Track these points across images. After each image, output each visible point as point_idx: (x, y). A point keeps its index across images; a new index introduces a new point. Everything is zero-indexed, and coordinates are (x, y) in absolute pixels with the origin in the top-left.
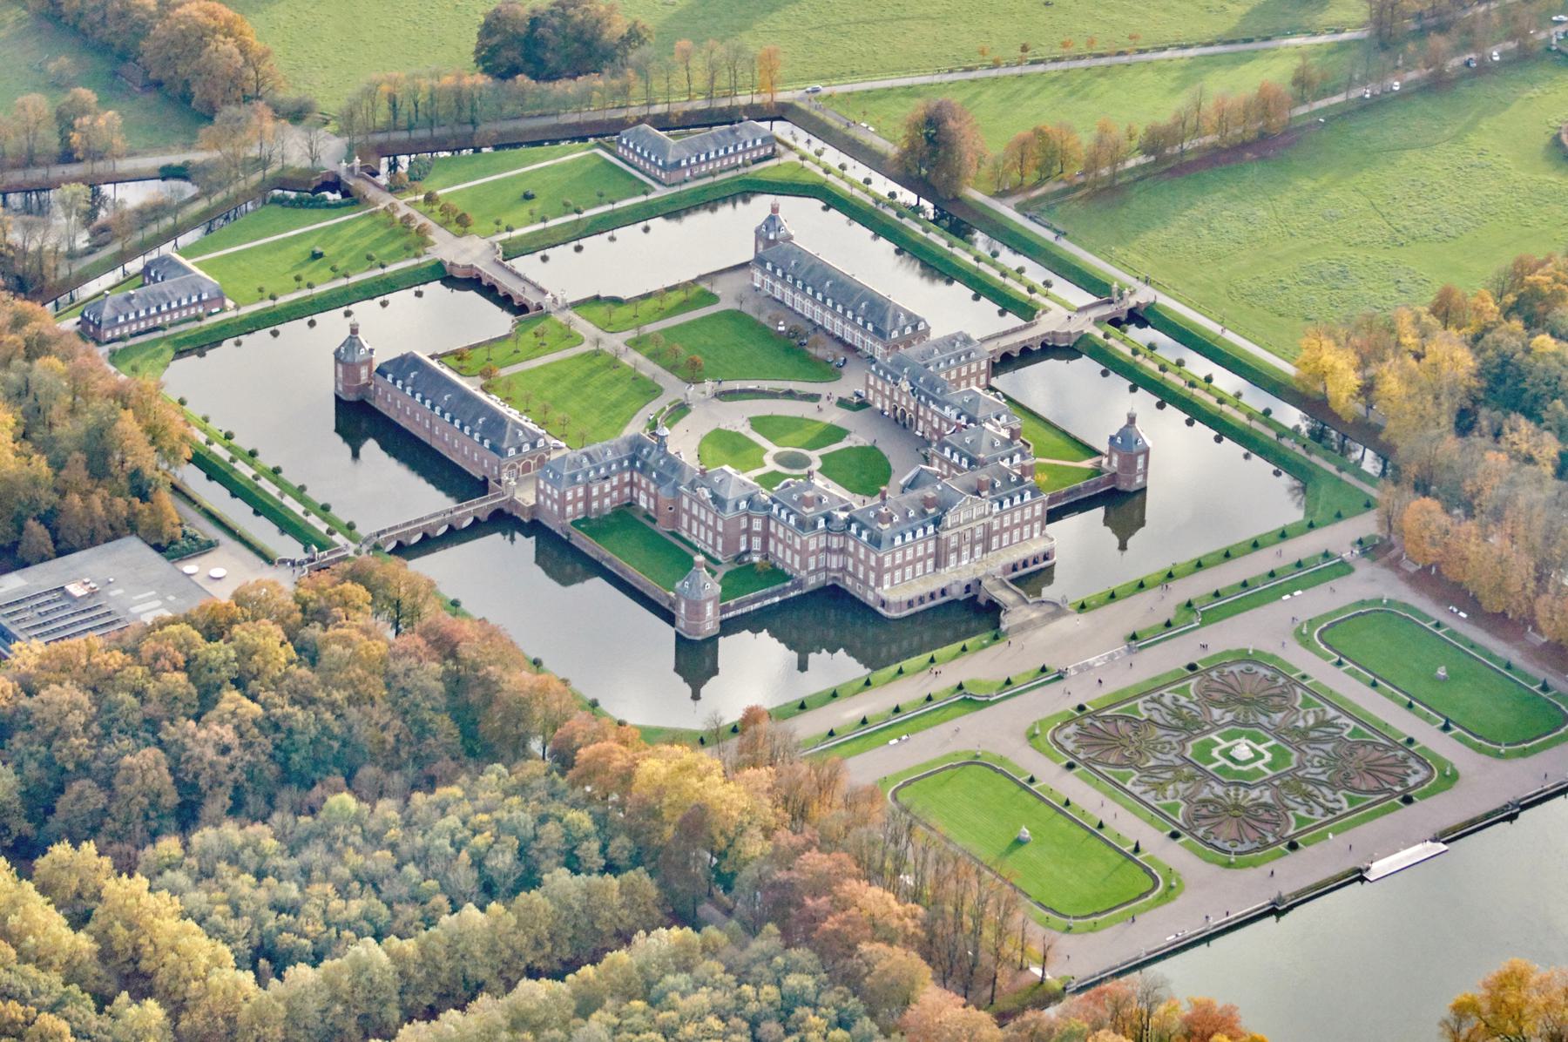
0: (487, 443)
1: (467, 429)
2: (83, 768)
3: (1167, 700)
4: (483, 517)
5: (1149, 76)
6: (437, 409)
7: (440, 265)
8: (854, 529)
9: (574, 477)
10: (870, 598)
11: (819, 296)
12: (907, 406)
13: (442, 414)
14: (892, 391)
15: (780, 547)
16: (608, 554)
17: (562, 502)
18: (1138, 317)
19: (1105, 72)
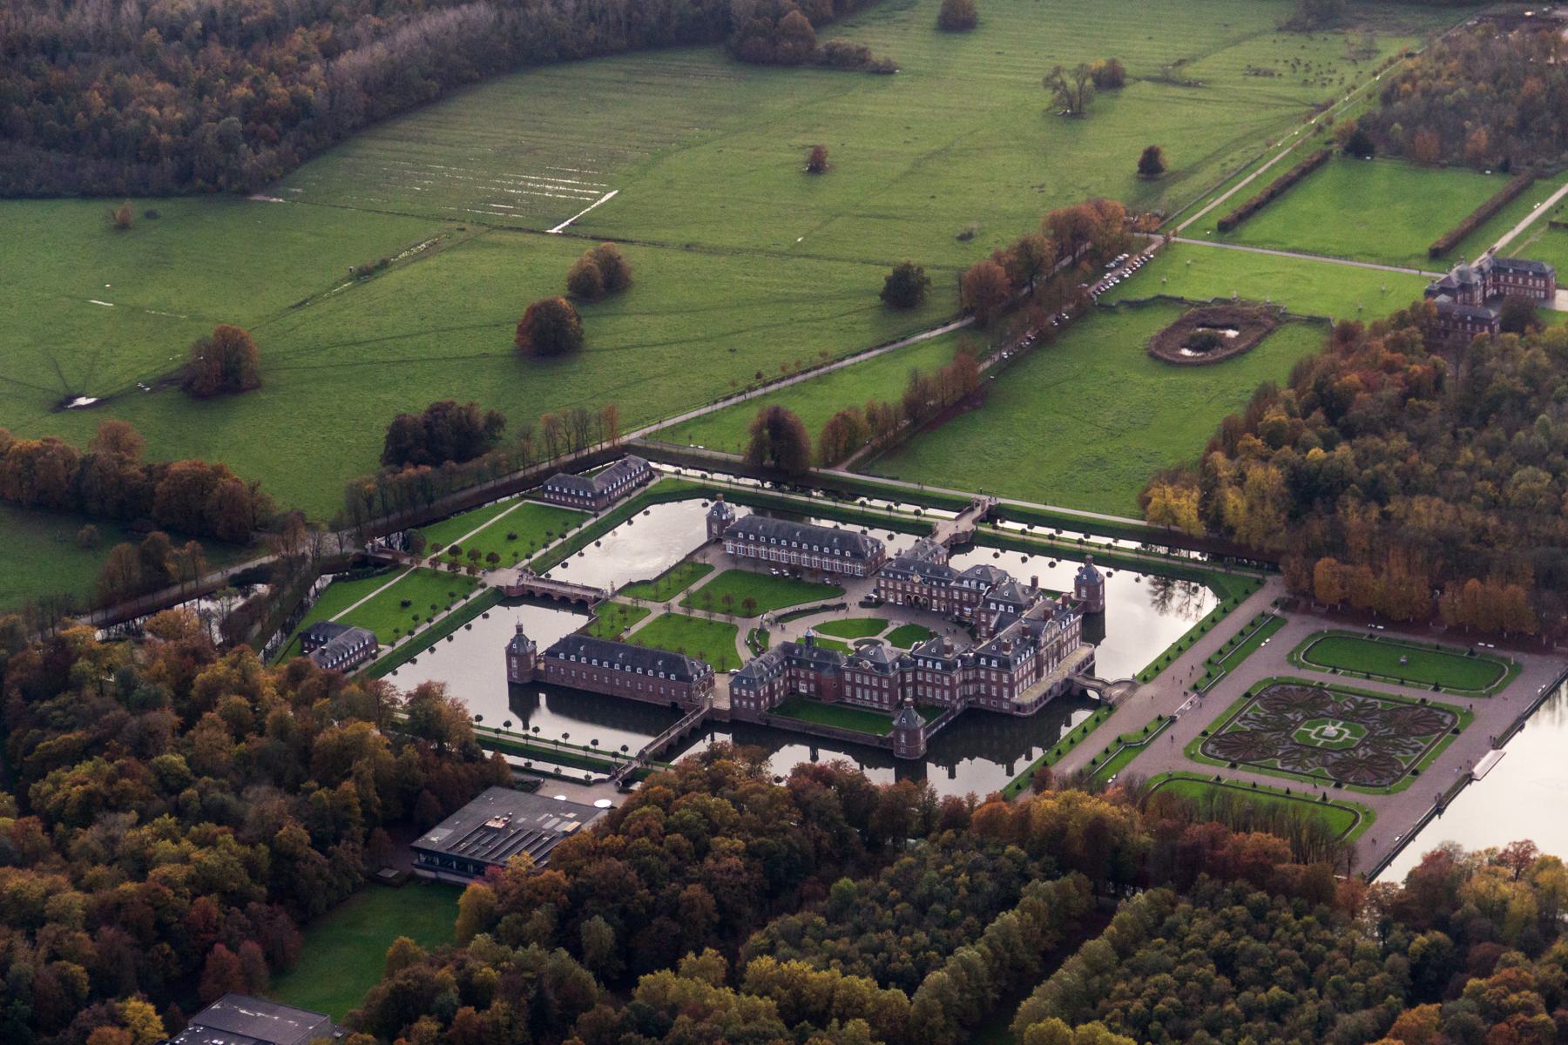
0: (673, 677)
1: (650, 673)
2: (653, 911)
3: (1250, 715)
4: (698, 725)
5: (848, 378)
6: (617, 666)
7: (498, 590)
8: (983, 661)
9: (761, 679)
10: (1006, 706)
11: (794, 544)
12: (921, 593)
13: (623, 667)
14: (904, 587)
15: (929, 690)
16: (811, 724)
17: (758, 699)
18: (993, 515)
19: (819, 380)
